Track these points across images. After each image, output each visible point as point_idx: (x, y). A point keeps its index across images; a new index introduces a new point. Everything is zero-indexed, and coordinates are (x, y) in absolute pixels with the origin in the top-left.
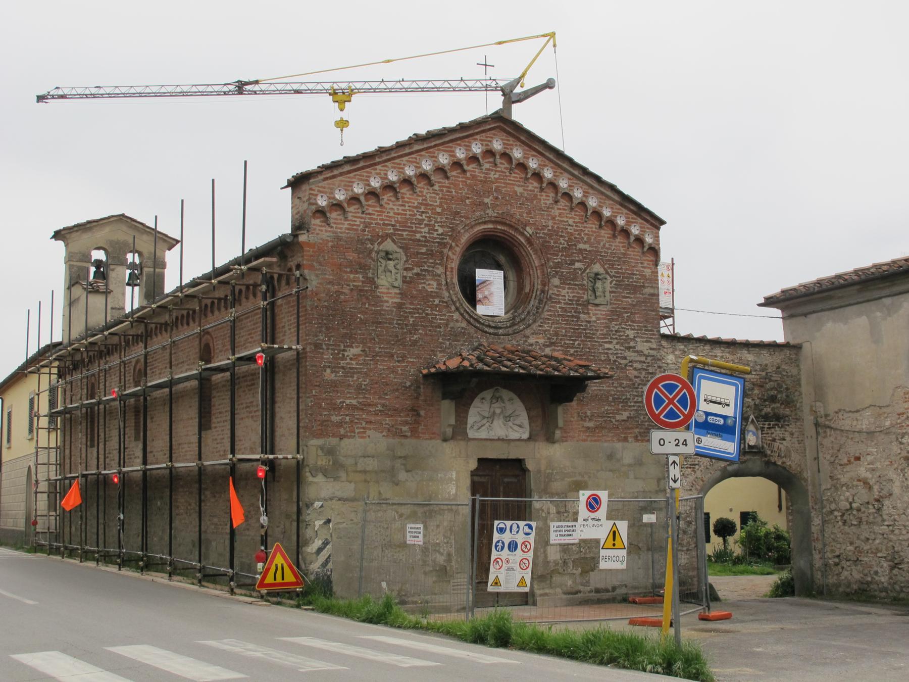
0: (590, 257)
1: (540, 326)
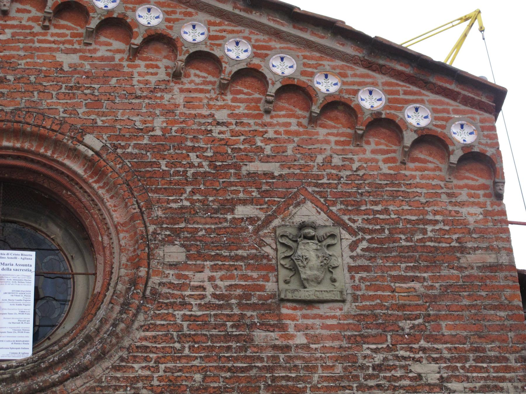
0: (278, 194)
1: (116, 368)
